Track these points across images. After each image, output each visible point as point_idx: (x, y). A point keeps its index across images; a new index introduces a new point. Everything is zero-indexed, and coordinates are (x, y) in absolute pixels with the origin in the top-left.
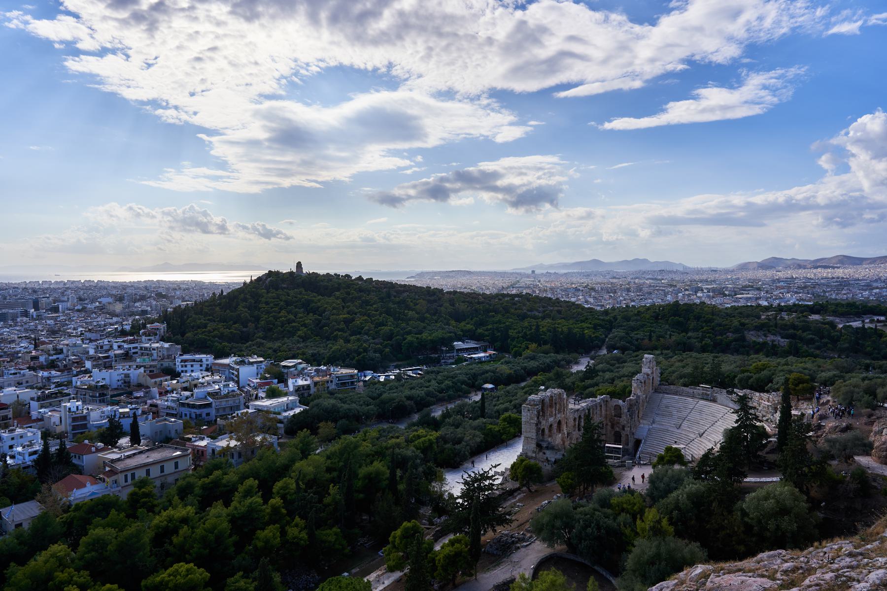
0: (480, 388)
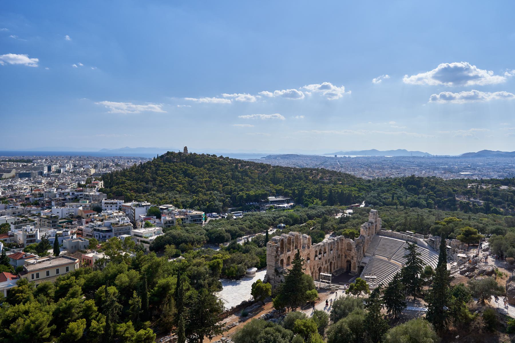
0: (275, 227)
